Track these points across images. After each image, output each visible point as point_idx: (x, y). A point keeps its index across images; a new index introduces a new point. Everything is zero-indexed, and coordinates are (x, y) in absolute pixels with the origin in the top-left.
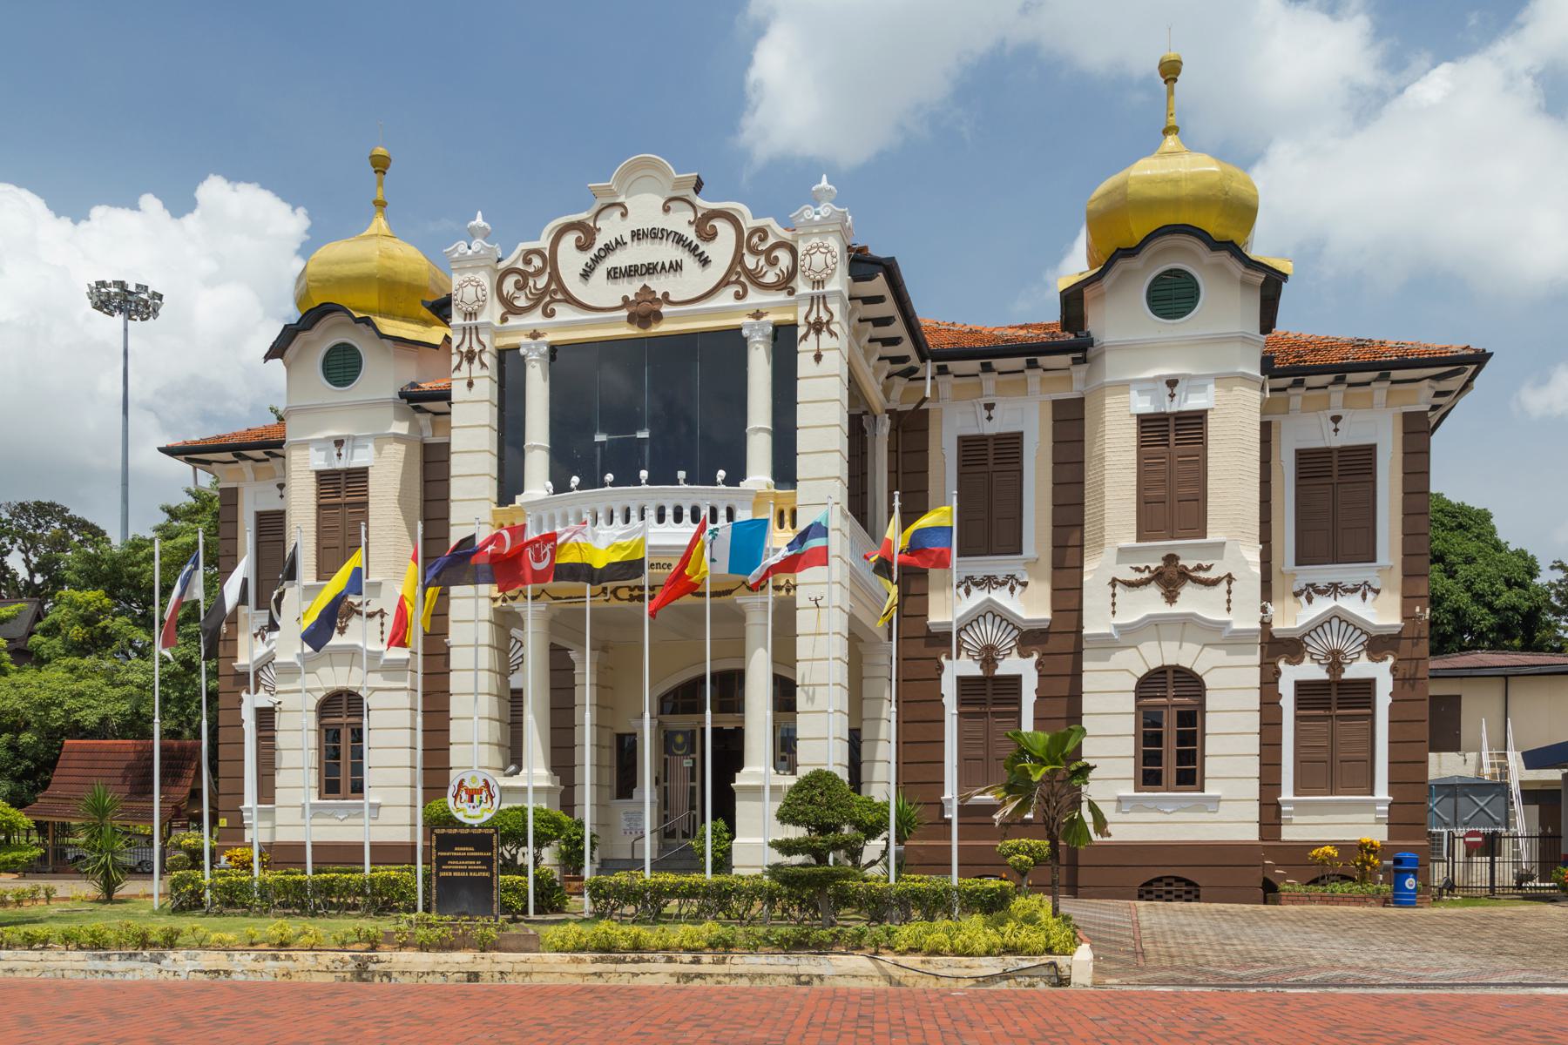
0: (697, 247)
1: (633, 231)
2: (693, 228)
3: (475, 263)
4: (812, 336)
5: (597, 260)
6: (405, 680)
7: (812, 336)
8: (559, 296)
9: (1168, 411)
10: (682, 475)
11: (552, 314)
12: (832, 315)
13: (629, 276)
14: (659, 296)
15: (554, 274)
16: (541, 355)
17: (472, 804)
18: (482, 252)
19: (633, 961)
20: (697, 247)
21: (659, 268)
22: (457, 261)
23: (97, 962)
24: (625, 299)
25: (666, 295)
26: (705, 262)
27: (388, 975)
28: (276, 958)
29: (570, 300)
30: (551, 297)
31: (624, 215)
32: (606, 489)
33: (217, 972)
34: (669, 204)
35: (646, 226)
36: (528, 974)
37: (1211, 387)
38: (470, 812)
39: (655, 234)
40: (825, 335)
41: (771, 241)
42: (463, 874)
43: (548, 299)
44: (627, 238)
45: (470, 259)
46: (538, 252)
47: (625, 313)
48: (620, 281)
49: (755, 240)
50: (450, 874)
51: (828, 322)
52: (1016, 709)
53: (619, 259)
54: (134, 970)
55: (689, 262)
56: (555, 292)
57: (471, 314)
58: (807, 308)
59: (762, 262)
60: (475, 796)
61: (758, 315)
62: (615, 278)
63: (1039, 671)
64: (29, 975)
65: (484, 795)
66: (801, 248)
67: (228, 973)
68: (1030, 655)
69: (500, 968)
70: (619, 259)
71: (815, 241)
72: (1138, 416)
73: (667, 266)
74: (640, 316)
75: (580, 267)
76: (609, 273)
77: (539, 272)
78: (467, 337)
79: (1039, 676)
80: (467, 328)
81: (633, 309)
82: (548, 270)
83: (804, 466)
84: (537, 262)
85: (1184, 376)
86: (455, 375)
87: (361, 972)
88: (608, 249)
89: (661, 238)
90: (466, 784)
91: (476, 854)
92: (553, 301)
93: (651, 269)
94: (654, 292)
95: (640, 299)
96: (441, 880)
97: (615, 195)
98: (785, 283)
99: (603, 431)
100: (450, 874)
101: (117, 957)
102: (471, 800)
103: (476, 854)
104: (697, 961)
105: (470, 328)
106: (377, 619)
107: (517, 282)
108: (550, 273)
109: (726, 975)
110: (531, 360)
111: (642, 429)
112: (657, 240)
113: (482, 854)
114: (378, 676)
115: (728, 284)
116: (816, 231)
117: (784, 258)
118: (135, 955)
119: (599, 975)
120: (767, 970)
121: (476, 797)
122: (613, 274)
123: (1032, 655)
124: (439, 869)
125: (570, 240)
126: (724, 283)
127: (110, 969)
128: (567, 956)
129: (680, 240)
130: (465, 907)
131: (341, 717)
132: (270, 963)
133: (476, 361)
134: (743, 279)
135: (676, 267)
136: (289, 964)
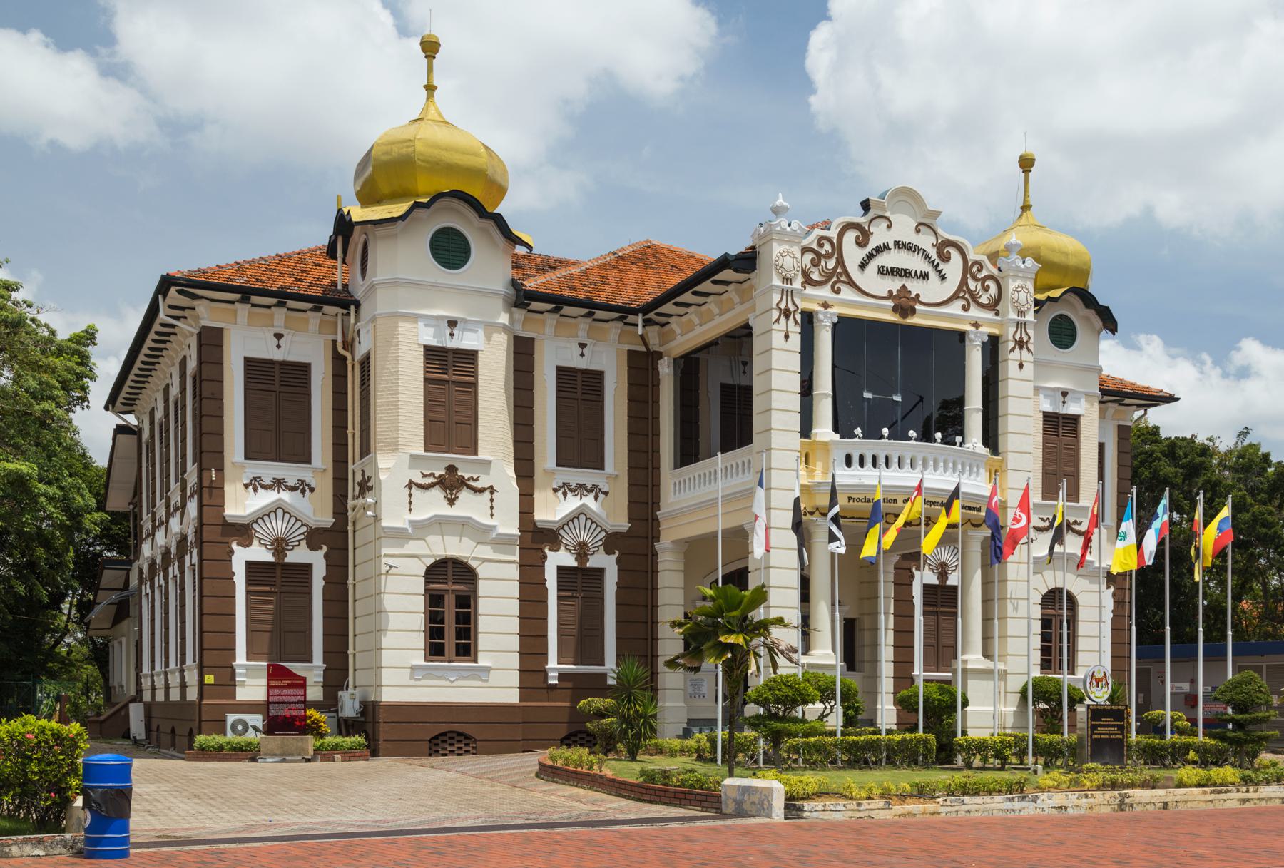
0: (938, 264)
2: (935, 250)
3: (792, 238)
4: (1017, 350)
5: (870, 256)
6: (515, 555)
7: (1017, 350)
8: (843, 278)
9: (1061, 412)
10: (938, 435)
11: (838, 291)
12: (1029, 338)
13: (893, 275)
14: (913, 295)
15: (840, 260)
18: (798, 231)
19: (1226, 792)
20: (938, 264)
21: (913, 274)
22: (778, 233)
23: (1008, 803)
24: (890, 292)
25: (918, 295)
26: (943, 278)
27: (1132, 805)
28: (1086, 796)
29: (851, 283)
30: (838, 278)
31: (889, 227)
32: (883, 441)
33: (1061, 807)
34: (920, 227)
35: (906, 240)
36: (1186, 802)
37: (1083, 400)
40: (1025, 351)
41: (984, 273)
43: (835, 279)
44: (891, 246)
45: (788, 234)
46: (829, 240)
47: (890, 303)
48: (886, 277)
49: (975, 269)
51: (1027, 342)
53: (886, 260)
54: (1024, 808)
55: (933, 275)
56: (840, 274)
57: (787, 279)
58: (1015, 329)
59: (979, 287)
61: (976, 325)
62: (882, 273)
64: (977, 814)
65: (1104, 682)
66: (1012, 285)
67: (1066, 808)
69: (1175, 799)
70: (886, 260)
71: (1019, 282)
72: (1044, 412)
74: (901, 308)
76: (879, 269)
77: (829, 256)
78: (785, 297)
80: (785, 290)
81: (897, 302)
82: (836, 256)
84: (827, 247)
85: (1073, 391)
86: (775, 326)
87: (1122, 806)
88: (878, 250)
89: (914, 252)
90: (1095, 674)
92: (839, 281)
93: (907, 273)
94: (910, 292)
95: (901, 295)
96: (1094, 741)
97: (884, 209)
98: (993, 306)
99: (869, 390)
101: (1016, 799)
102: (1098, 686)
104: (1248, 791)
105: (787, 291)
107: (812, 260)
108: (837, 259)
109: (1259, 799)
110: (826, 325)
111: (896, 394)
112: (911, 253)
113: (1117, 723)
114: (488, 548)
115: (958, 297)
116: (1020, 275)
117: (993, 290)
118: (1025, 797)
119: (1211, 801)
120: (1273, 795)
122: (882, 271)
124: (1093, 733)
125: (851, 236)
126: (955, 297)
127: (1015, 808)
128: (1201, 789)
129: (927, 257)
130: (1107, 759)
131: (446, 583)
132: (1085, 800)
133: (791, 318)
134: (967, 296)
135: (925, 276)
136: (1092, 800)
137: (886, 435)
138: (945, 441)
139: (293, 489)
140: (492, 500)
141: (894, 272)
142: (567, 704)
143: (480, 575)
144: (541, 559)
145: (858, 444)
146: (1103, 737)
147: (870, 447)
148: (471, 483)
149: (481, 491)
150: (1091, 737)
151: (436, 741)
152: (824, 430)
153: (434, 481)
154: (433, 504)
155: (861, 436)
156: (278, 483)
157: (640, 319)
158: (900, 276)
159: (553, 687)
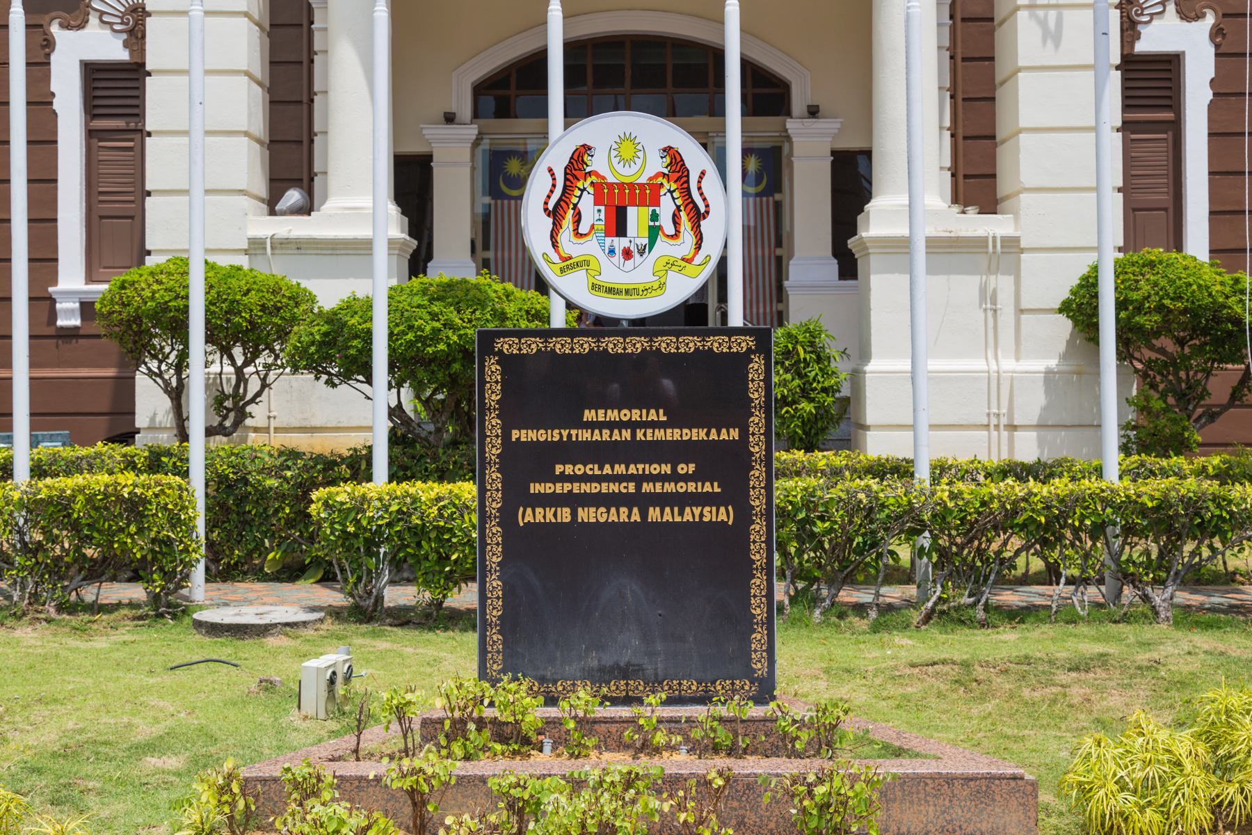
17: (620, 243)
38: (613, 272)
42: (621, 515)
50: (565, 515)
52: (1168, 115)
60: (632, 212)
63: (1217, 46)
65: (667, 207)
68: (1199, 16)
79: (1217, 55)
90: (597, 163)
91: (674, 434)
100: (565, 515)
102: (618, 226)
103: (674, 434)
113: (698, 434)
121: (637, 217)
123: (1203, 16)
124: (516, 496)
130: (628, 647)
142: (111, 372)
144: (44, 47)
146: (587, 515)
150: (507, 517)
159: (70, 334)
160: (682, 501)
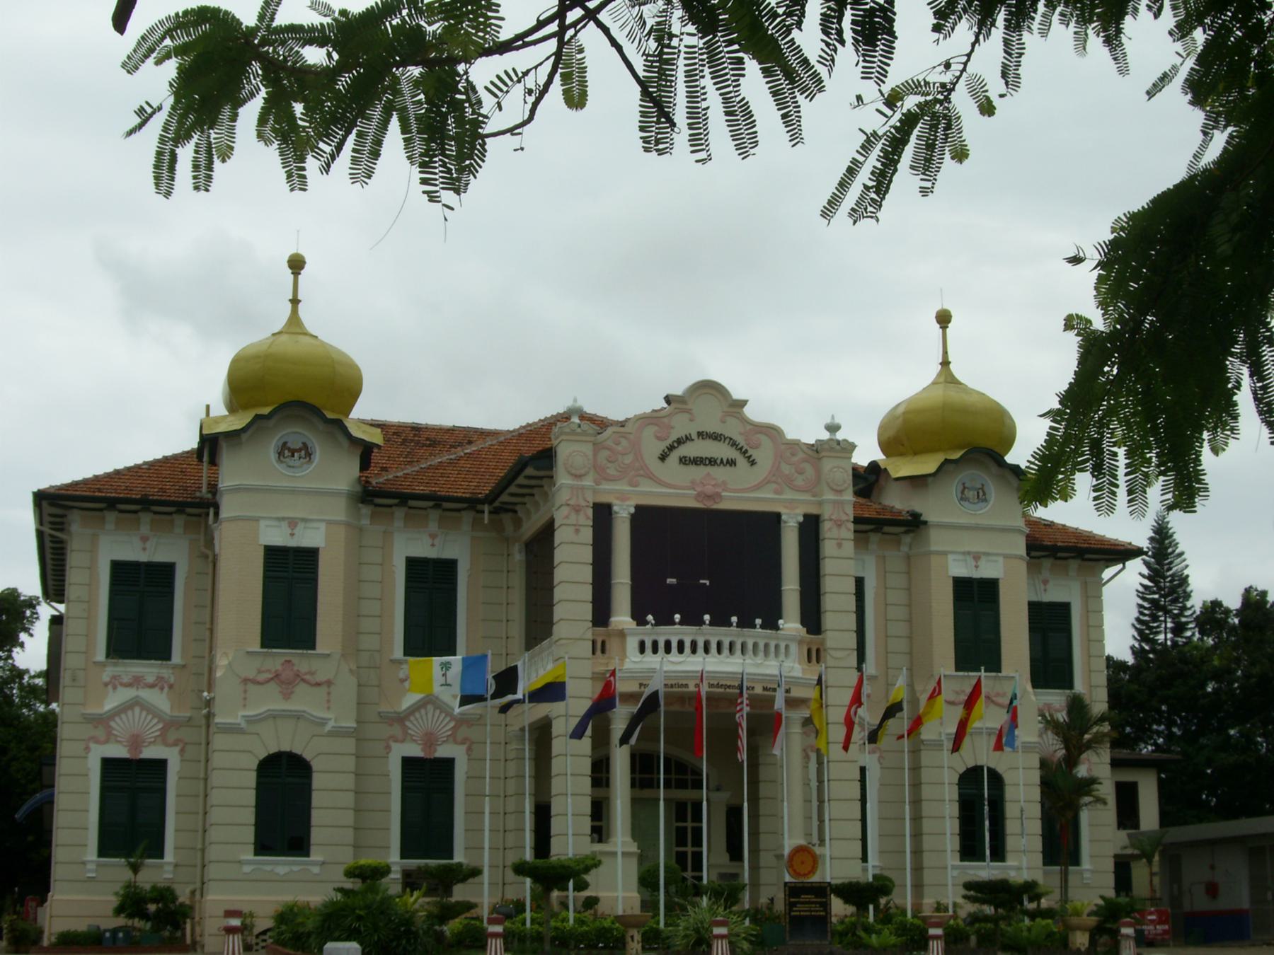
1: (698, 432)
5: (671, 448)
13: (696, 464)
16: (629, 513)
20: (746, 451)
21: (718, 462)
26: (753, 463)
35: (710, 429)
39: (716, 437)
42: (808, 913)
44: (694, 436)
53: (688, 450)
55: (741, 461)
59: (793, 471)
62: (685, 464)
70: (688, 450)
73: (725, 461)
75: (658, 452)
76: (681, 460)
83: (829, 620)
88: (680, 442)
93: (712, 462)
96: (793, 919)
100: (798, 913)
106: (324, 689)
122: (684, 461)
124: (791, 910)
129: (734, 444)
135: (732, 463)
137: (677, 620)
138: (739, 625)
139: (152, 686)
140: (329, 694)
141: (697, 461)
143: (315, 768)
145: (652, 632)
146: (802, 913)
147: (664, 633)
148: (307, 677)
149: (318, 684)
150: (790, 913)
151: (264, 937)
152: (622, 618)
153: (270, 676)
154: (270, 701)
155: (653, 622)
156: (137, 682)
157: (486, 508)
158: (705, 465)
160: (817, 911)
